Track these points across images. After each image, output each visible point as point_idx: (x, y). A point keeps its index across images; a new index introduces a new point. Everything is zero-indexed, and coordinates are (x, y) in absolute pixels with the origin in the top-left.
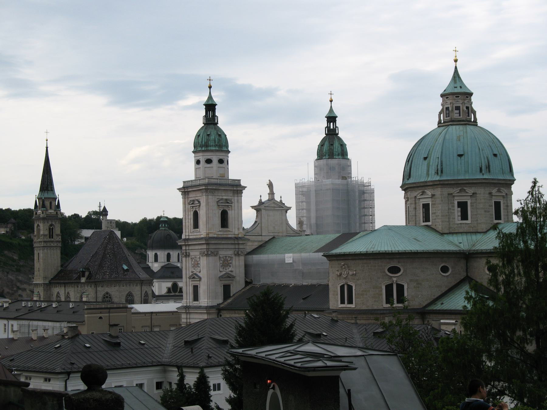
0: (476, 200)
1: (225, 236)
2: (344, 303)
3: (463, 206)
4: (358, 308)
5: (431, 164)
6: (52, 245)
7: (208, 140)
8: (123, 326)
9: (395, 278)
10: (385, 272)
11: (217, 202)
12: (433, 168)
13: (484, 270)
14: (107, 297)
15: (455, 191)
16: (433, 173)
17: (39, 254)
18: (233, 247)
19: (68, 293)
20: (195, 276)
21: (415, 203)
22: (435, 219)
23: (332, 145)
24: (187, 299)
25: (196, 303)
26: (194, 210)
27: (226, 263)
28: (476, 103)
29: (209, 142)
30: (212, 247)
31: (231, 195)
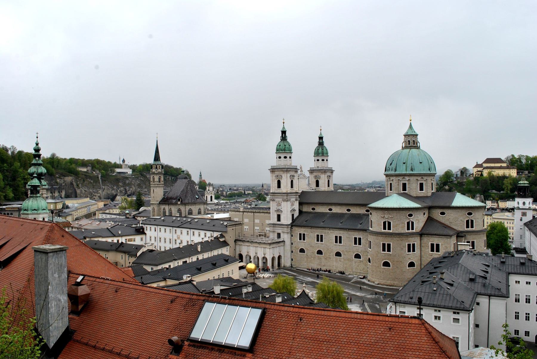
2: (386, 229)
3: (421, 185)
4: (394, 232)
5: (408, 165)
6: (160, 186)
9: (411, 219)
12: (409, 168)
15: (419, 178)
16: (410, 170)
18: (295, 197)
19: (171, 208)
21: (398, 183)
25: (279, 223)
27: (292, 205)
28: (420, 139)
30: (289, 197)
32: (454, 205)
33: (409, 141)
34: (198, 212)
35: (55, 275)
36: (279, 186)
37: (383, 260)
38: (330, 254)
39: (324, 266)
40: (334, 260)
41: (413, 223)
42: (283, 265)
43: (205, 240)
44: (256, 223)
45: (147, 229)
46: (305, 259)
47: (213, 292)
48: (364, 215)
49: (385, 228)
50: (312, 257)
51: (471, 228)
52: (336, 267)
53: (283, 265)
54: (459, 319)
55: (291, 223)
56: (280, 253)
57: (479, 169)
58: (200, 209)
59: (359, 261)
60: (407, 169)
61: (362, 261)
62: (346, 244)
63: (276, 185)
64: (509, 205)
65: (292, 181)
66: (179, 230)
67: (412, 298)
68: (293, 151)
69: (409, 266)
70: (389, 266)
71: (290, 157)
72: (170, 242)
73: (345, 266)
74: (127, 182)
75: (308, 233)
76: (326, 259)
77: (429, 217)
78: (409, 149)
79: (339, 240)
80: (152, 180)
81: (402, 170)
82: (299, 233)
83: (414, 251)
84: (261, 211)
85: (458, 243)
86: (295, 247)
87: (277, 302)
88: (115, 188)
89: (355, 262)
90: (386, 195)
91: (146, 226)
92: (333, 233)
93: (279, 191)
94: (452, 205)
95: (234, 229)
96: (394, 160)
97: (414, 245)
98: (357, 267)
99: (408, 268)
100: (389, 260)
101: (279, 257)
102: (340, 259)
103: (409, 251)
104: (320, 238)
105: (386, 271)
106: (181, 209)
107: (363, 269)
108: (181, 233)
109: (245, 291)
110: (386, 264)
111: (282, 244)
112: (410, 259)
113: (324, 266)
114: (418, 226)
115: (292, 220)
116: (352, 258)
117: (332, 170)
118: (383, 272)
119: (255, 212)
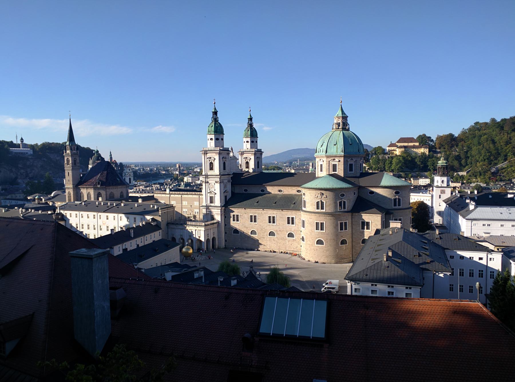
0: (356, 163)
1: (225, 174)
3: (351, 165)
4: (327, 211)
5: (338, 147)
8: (172, 216)
10: (339, 196)
11: (223, 158)
13: (367, 193)
14: (112, 194)
16: (340, 151)
17: (68, 173)
20: (212, 192)
22: (339, 171)
24: (206, 202)
26: (210, 162)
27: (225, 186)
29: (218, 130)
31: (226, 154)
32: (382, 185)
33: (339, 123)
34: (120, 195)
35: (99, 281)
36: (211, 168)
37: (317, 238)
38: (264, 234)
41: (344, 202)
42: (217, 247)
43: (136, 225)
44: (184, 206)
45: (121, 219)
47: (165, 279)
48: (296, 195)
49: (318, 208)
51: (398, 206)
52: (270, 247)
53: (217, 247)
54: (411, 294)
55: (224, 205)
56: (214, 235)
57: (393, 148)
58: (122, 192)
59: (293, 240)
60: (338, 151)
61: (296, 240)
62: (279, 224)
64: (421, 182)
65: (224, 163)
66: (104, 215)
67: (367, 275)
68: (224, 133)
69: (341, 244)
70: (323, 244)
71: (222, 139)
72: (95, 229)
73: (279, 245)
74: (28, 163)
77: (358, 196)
78: (339, 131)
79: (272, 220)
80: (66, 162)
81: (333, 151)
83: (346, 229)
84: (188, 193)
85: (390, 221)
87: (232, 285)
88: (14, 170)
89: (289, 241)
90: (317, 176)
91: (66, 212)
92: (267, 213)
94: (381, 185)
95: (166, 213)
96: (325, 142)
97: (346, 223)
98: (291, 246)
99: (340, 245)
100: (322, 238)
101: (214, 239)
103: (341, 229)
104: (253, 219)
105: (319, 248)
106: (101, 192)
107: (296, 248)
108: (107, 219)
109: (196, 275)
110: (319, 242)
111: (216, 225)
112: (342, 236)
114: (349, 205)
115: (225, 201)
116: (286, 237)
117: (261, 151)
118: (317, 249)
119: (183, 194)
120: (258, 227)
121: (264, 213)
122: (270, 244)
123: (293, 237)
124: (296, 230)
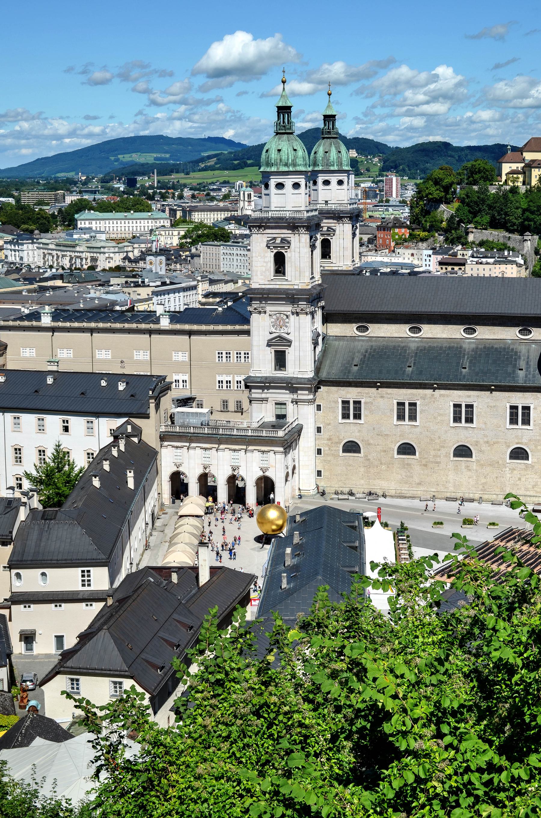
7: (296, 157)
23: (340, 152)
25: (280, 374)
26: (275, 251)
29: (297, 160)
39: (419, 484)
40: (451, 466)
46: (362, 469)
50: (381, 464)
59: (523, 467)
62: (485, 424)
63: (271, 265)
73: (483, 481)
75: (369, 400)
76: (425, 465)
82: (340, 401)
86: (330, 439)
93: (280, 284)
98: (518, 482)
102: (468, 464)
113: (419, 484)
120: (421, 433)
121: (440, 395)
122: (457, 479)
123: (527, 459)
124: (535, 440)
